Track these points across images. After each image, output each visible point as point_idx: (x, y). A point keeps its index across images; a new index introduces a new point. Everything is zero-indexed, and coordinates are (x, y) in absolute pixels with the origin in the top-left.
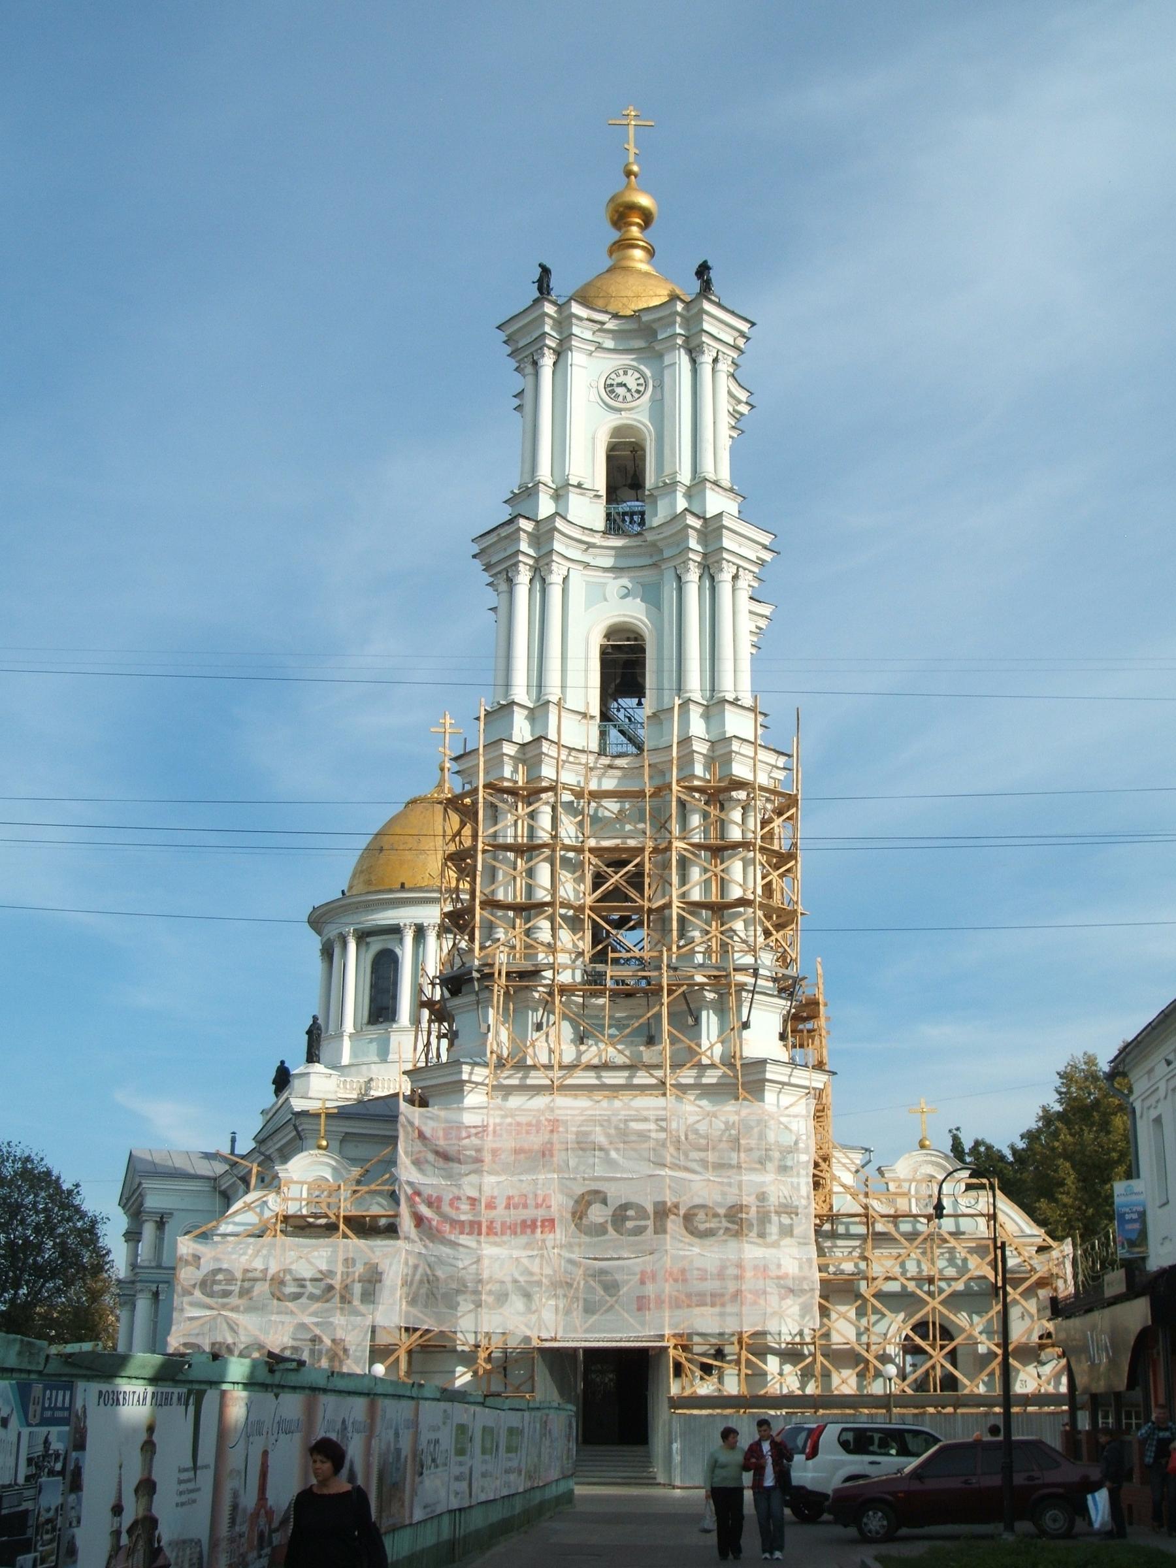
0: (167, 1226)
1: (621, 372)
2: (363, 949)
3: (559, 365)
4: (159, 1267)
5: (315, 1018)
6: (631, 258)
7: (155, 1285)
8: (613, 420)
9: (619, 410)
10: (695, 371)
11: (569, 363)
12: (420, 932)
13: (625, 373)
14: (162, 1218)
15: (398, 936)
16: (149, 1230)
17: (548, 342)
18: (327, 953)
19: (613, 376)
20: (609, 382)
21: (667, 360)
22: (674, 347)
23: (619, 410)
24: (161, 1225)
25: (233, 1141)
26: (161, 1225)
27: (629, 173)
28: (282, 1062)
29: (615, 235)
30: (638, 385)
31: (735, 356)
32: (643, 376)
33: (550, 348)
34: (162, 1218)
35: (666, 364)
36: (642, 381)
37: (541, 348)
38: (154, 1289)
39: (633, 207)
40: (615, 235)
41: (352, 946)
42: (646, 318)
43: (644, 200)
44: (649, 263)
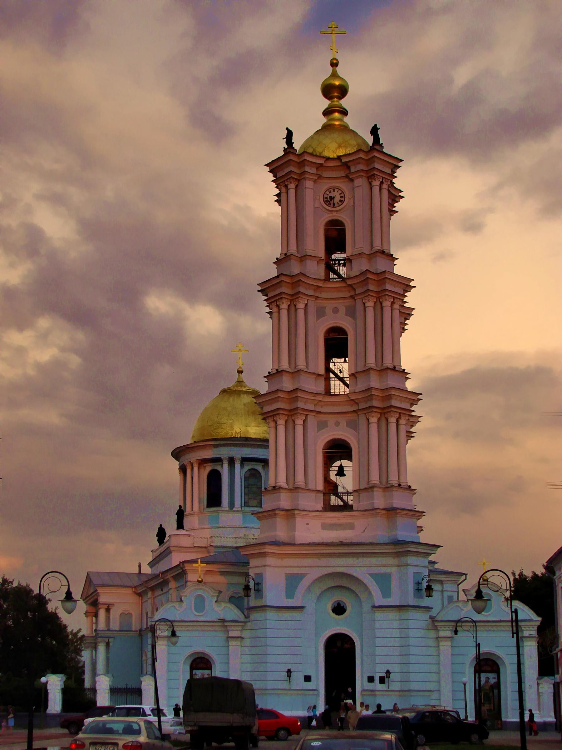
0: (111, 611)
1: (332, 190)
2: (202, 470)
4: (109, 630)
5: (180, 506)
7: (108, 639)
9: (331, 211)
12: (231, 461)
13: (334, 191)
14: (108, 607)
15: (220, 463)
16: (102, 613)
18: (183, 470)
19: (327, 192)
20: (326, 196)
23: (331, 211)
24: (108, 610)
25: (140, 567)
26: (108, 610)
28: (161, 525)
30: (341, 197)
34: (108, 607)
38: (107, 641)
41: (196, 469)
42: (344, 160)
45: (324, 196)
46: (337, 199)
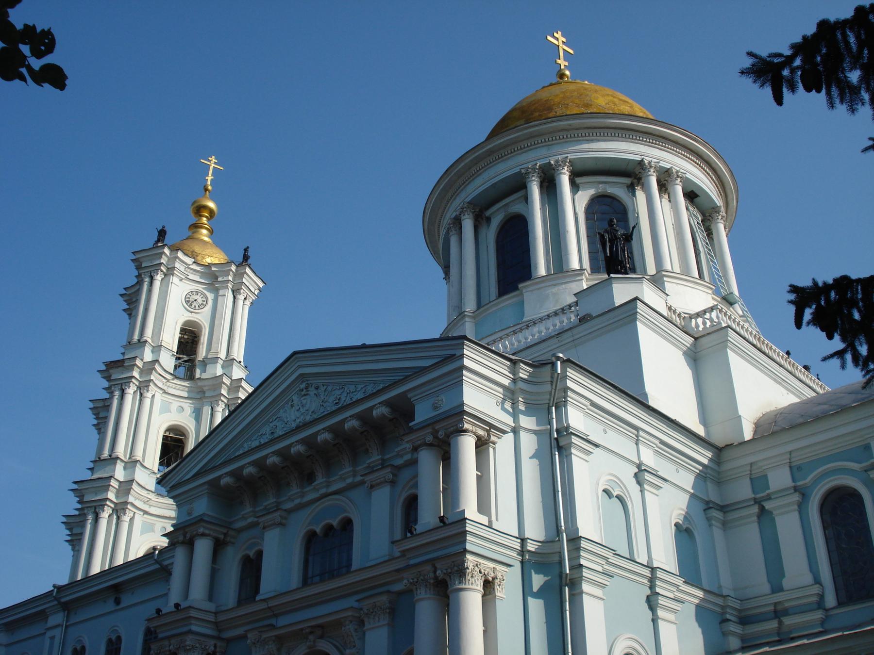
1: (194, 293)
3: (164, 281)
6: (201, 234)
8: (187, 316)
10: (234, 302)
11: (171, 281)
17: (162, 268)
19: (190, 294)
21: (221, 292)
22: (227, 287)
23: (192, 312)
27: (206, 190)
29: (193, 219)
31: (254, 299)
32: (207, 298)
33: (162, 271)
35: (220, 294)
36: (205, 299)
37: (158, 270)
39: (205, 207)
40: (193, 219)
43: (211, 205)
44: (209, 237)
45: (186, 295)
46: (200, 301)
